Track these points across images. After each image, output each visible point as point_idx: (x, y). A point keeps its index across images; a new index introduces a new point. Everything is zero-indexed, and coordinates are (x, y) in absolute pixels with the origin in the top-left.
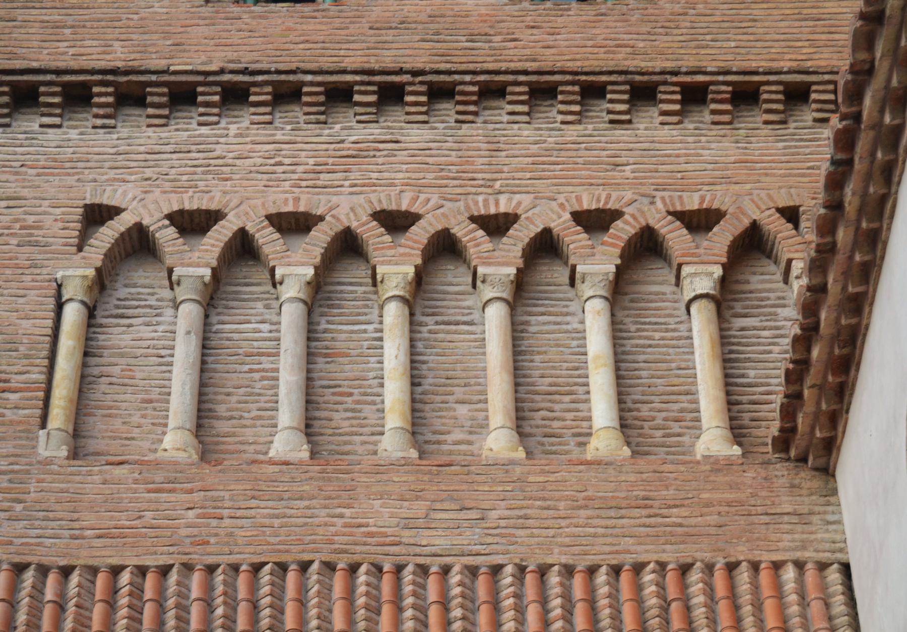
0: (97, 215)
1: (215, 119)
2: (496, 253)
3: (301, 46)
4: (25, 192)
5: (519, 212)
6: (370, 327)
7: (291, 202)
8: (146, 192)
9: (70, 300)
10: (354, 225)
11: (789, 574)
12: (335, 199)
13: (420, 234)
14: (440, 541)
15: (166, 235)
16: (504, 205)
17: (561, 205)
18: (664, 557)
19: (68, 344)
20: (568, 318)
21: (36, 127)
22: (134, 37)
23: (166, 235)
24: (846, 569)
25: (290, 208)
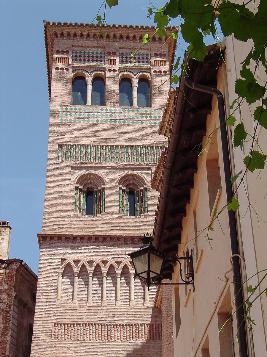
0: (63, 260)
1: (79, 242)
2: (119, 269)
3: (92, 227)
4: (52, 256)
5: (122, 261)
6: (101, 280)
7: (90, 259)
8: (70, 256)
9: (60, 276)
10: (99, 263)
11: (154, 326)
12: (96, 258)
13: (108, 265)
14: (109, 320)
15: (73, 264)
16: (120, 260)
17: (128, 260)
18: (138, 323)
19: (60, 284)
20: (128, 279)
21: (54, 243)
22: (67, 224)
23: (73, 264)
24: (161, 325)
25: (89, 260)
